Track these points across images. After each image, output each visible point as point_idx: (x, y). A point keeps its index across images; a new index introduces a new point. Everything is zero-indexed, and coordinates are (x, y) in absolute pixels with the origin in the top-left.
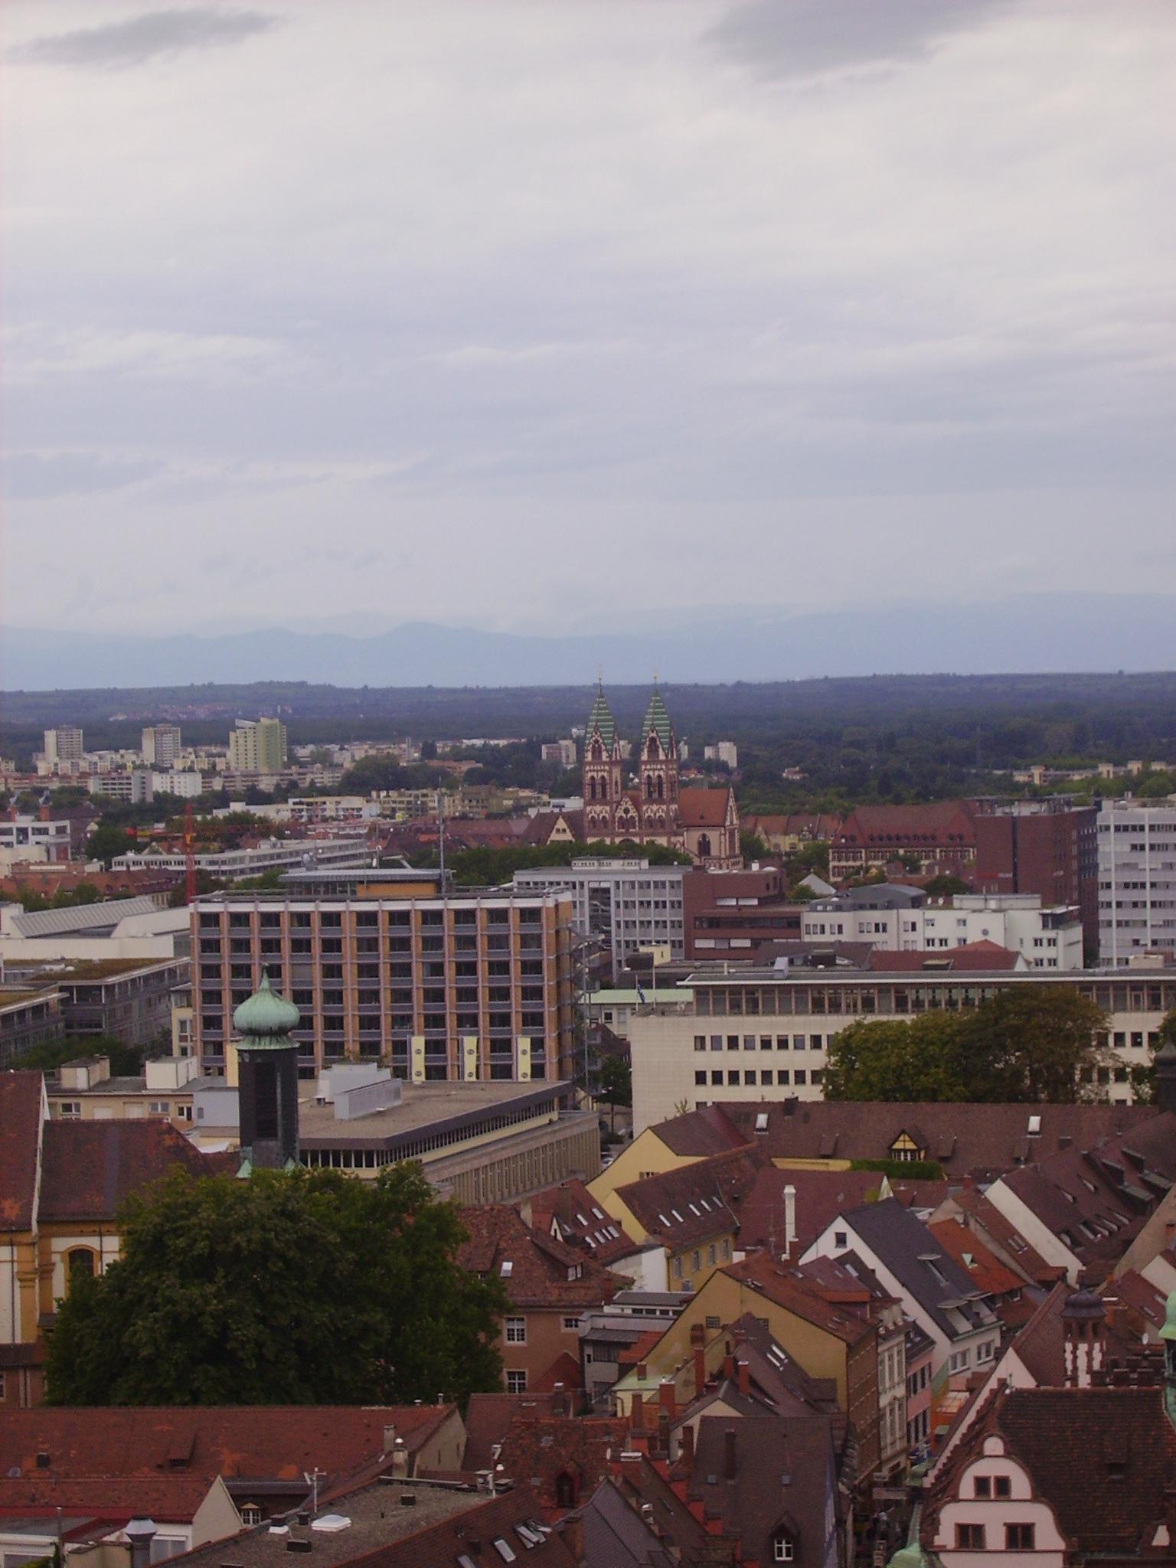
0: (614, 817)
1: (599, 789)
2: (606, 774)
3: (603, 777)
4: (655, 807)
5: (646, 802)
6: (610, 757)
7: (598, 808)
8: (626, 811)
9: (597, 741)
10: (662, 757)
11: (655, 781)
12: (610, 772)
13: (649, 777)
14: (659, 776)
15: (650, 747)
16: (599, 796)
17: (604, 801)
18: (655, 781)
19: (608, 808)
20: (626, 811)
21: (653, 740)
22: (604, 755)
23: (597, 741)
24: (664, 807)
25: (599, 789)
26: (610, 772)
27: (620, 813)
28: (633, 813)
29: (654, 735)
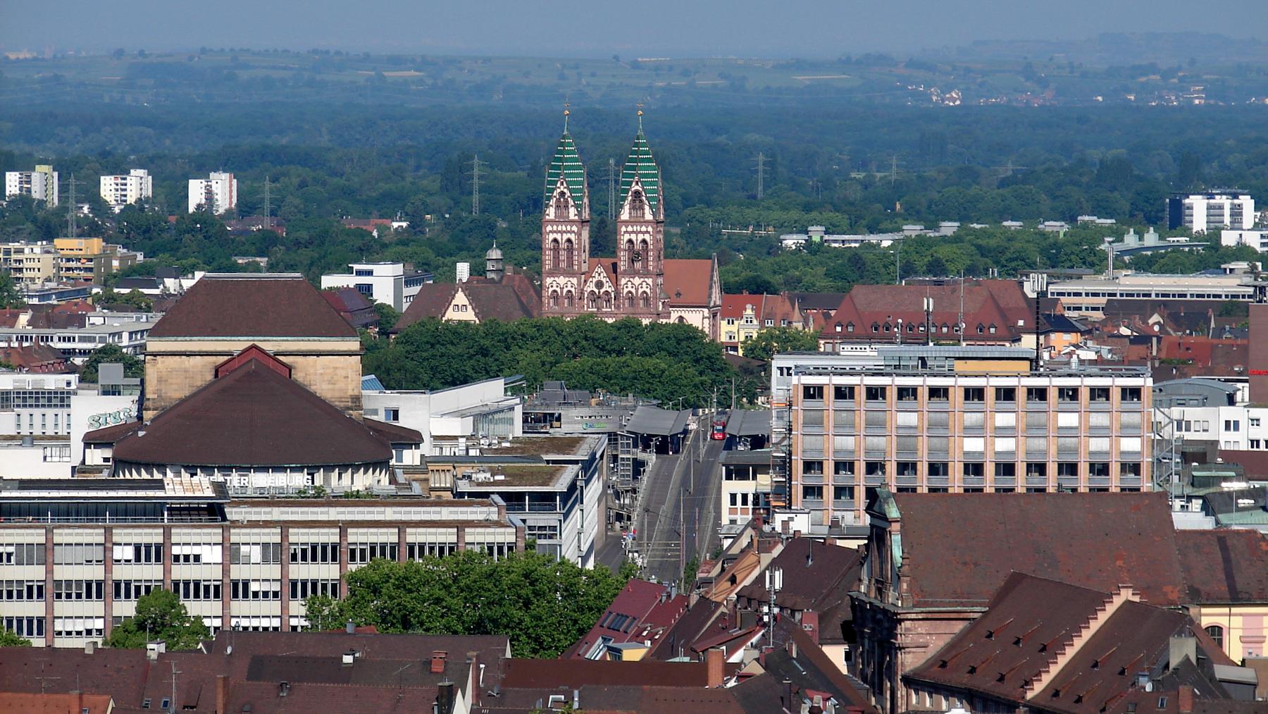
0: (582, 293)
1: (563, 255)
2: (573, 237)
3: (569, 241)
4: (637, 281)
5: (625, 273)
7: (562, 280)
8: (599, 285)
9: (562, 194)
11: (638, 246)
12: (579, 234)
14: (644, 241)
15: (634, 201)
17: (569, 273)
18: (638, 246)
19: (575, 281)
20: (599, 285)
21: (637, 193)
23: (562, 194)
24: (650, 281)
25: (563, 255)
26: (579, 234)
27: (591, 287)
28: (608, 287)
29: (638, 188)
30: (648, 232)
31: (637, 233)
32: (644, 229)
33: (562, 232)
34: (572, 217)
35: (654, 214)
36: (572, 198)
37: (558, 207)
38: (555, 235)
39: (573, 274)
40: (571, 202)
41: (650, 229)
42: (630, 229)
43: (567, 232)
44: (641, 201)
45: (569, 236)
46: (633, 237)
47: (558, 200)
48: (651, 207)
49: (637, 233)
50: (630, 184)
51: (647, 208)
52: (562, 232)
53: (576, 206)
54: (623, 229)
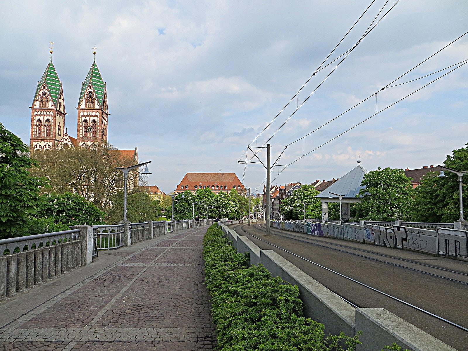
1: (44, 129)
2: (50, 118)
3: (48, 120)
6: (55, 105)
7: (43, 144)
10: (97, 107)
11: (90, 124)
13: (85, 121)
14: (94, 121)
16: (44, 135)
18: (90, 124)
22: (50, 103)
23: (45, 93)
25: (44, 129)
29: (90, 90)
30: (96, 116)
31: (90, 116)
32: (94, 114)
33: (44, 116)
34: (50, 107)
35: (100, 106)
36: (51, 96)
37: (41, 101)
38: (39, 117)
39: (50, 140)
40: (50, 98)
41: (98, 114)
42: (85, 114)
43: (48, 115)
44: (93, 98)
45: (48, 117)
46: (87, 118)
47: (42, 97)
48: (98, 101)
49: (90, 116)
50: (86, 89)
51: (96, 102)
52: (44, 116)
53: (53, 101)
54: (81, 114)
